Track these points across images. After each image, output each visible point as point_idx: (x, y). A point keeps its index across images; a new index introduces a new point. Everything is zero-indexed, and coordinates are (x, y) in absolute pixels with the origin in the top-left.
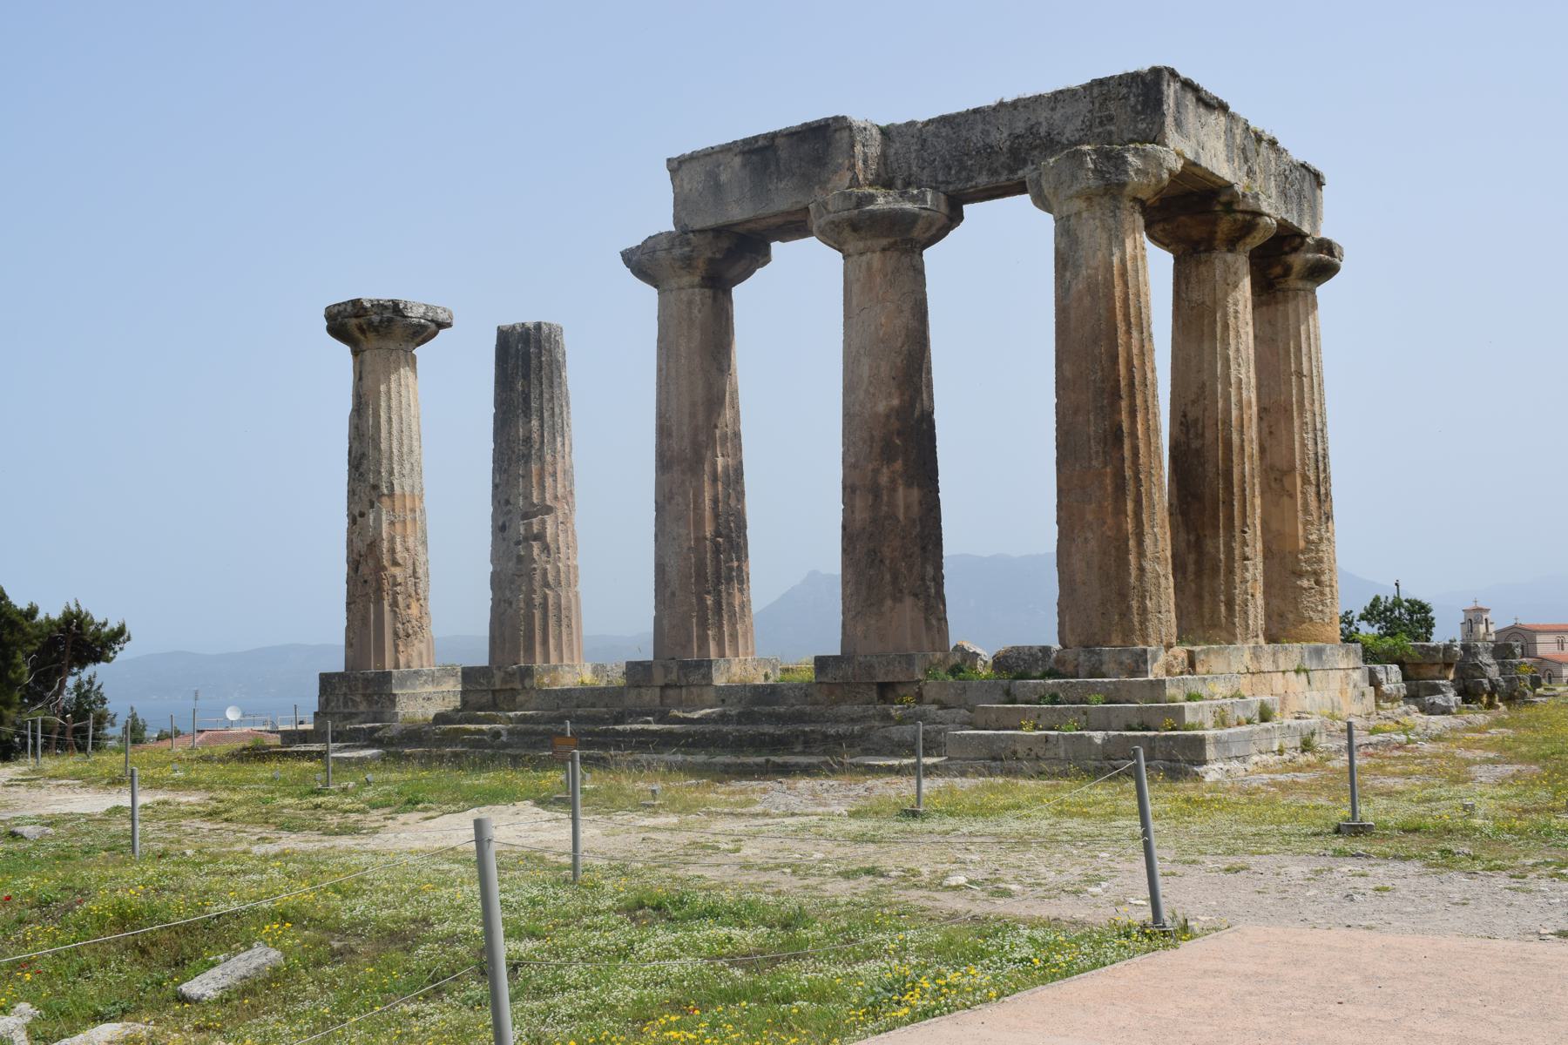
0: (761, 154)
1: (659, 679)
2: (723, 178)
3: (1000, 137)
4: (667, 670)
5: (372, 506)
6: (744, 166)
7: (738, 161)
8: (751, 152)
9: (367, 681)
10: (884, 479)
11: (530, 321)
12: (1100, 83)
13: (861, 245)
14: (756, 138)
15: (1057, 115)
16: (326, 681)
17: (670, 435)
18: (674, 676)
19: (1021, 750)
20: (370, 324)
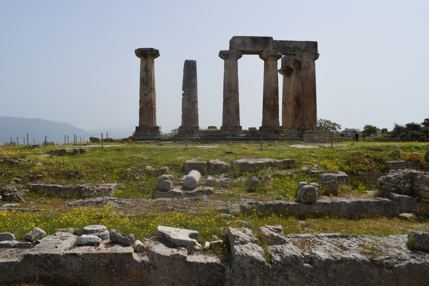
0: (255, 40)
1: (230, 129)
2: (246, 42)
3: (291, 46)
4: (232, 128)
5: (150, 92)
6: (251, 41)
7: (249, 40)
8: (252, 39)
9: (151, 128)
10: (276, 98)
11: (194, 60)
12: (308, 42)
13: (272, 59)
14: (254, 37)
15: (300, 45)
16: (137, 127)
17: (231, 86)
18: (233, 129)
19: (316, 140)
20: (153, 54)
